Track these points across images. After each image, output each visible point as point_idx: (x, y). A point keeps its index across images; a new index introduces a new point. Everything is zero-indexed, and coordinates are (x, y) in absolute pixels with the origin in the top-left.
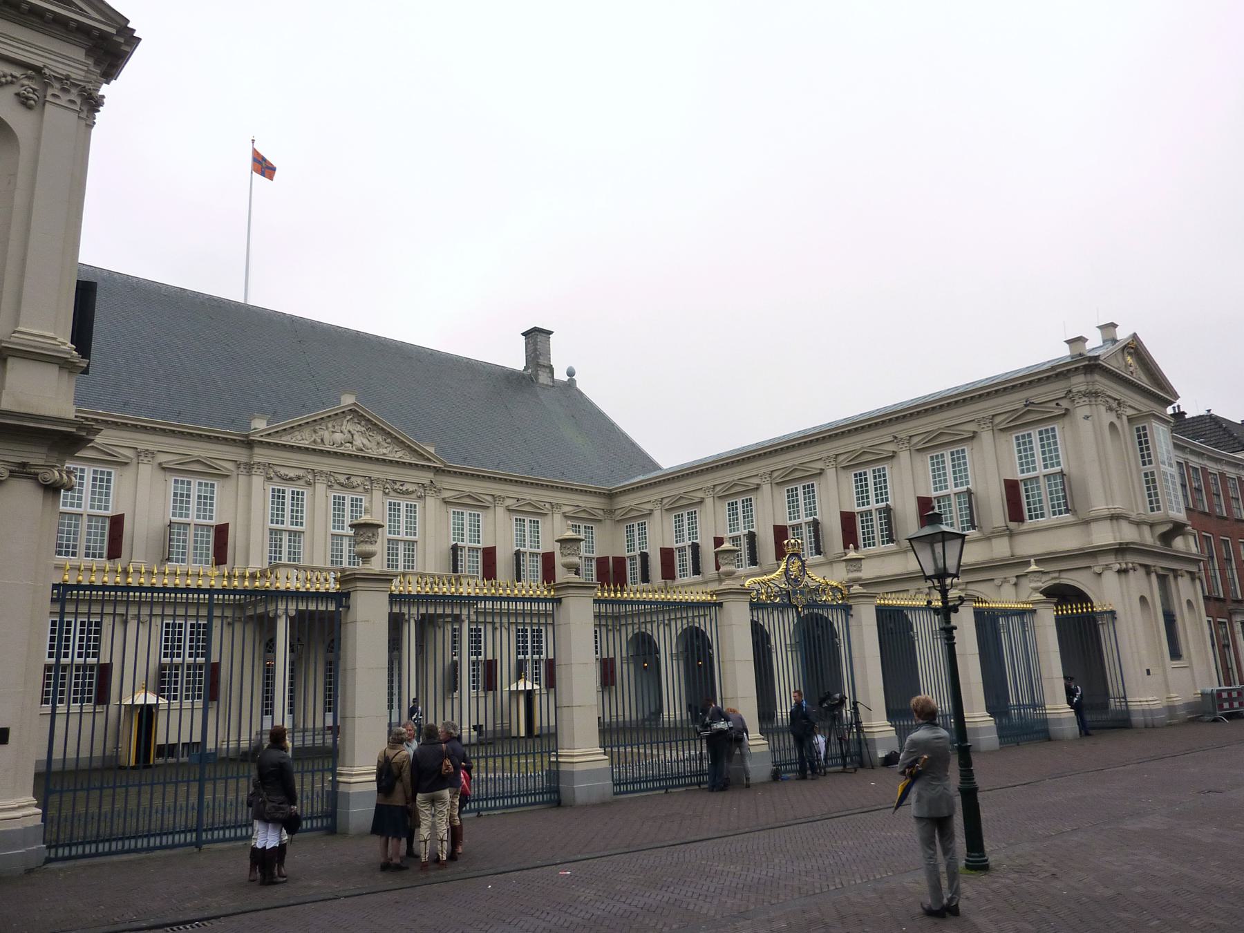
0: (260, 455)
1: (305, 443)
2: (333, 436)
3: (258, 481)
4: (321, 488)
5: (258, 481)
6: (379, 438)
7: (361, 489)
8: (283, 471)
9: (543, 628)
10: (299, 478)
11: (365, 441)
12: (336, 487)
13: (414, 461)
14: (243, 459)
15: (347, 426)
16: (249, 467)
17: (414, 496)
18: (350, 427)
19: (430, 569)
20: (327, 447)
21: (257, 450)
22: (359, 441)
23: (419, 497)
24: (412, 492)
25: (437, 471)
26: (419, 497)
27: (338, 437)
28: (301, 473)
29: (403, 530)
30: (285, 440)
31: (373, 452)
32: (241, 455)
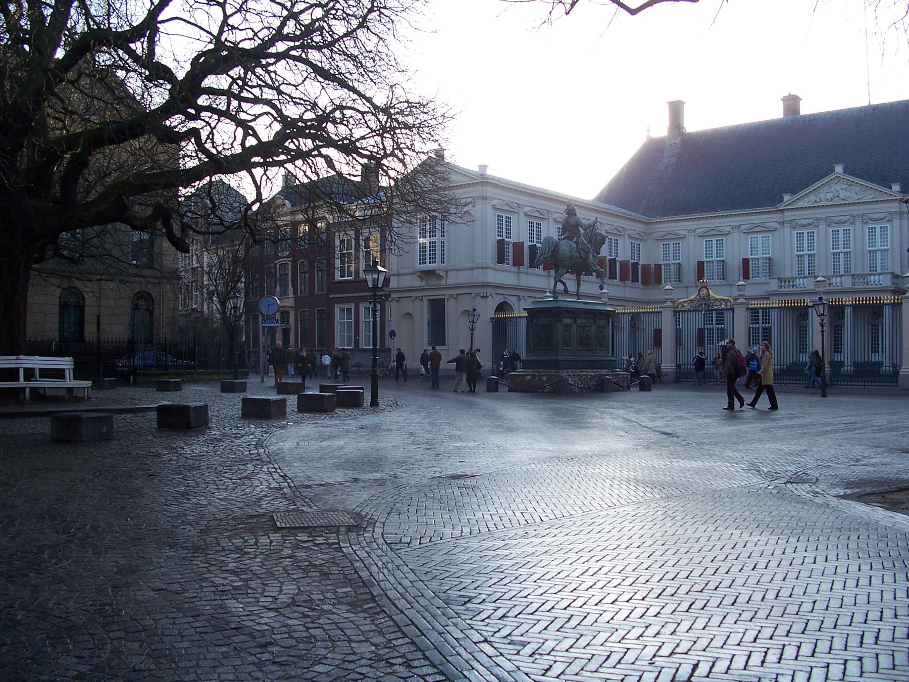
0: (788, 216)
3: (787, 230)
4: (822, 227)
5: (787, 230)
6: (858, 188)
8: (800, 222)
11: (849, 194)
14: (779, 220)
16: (783, 223)
18: (837, 187)
21: (786, 214)
24: (882, 219)
26: (889, 221)
27: (829, 196)
28: (810, 221)
30: (800, 204)
32: (777, 217)
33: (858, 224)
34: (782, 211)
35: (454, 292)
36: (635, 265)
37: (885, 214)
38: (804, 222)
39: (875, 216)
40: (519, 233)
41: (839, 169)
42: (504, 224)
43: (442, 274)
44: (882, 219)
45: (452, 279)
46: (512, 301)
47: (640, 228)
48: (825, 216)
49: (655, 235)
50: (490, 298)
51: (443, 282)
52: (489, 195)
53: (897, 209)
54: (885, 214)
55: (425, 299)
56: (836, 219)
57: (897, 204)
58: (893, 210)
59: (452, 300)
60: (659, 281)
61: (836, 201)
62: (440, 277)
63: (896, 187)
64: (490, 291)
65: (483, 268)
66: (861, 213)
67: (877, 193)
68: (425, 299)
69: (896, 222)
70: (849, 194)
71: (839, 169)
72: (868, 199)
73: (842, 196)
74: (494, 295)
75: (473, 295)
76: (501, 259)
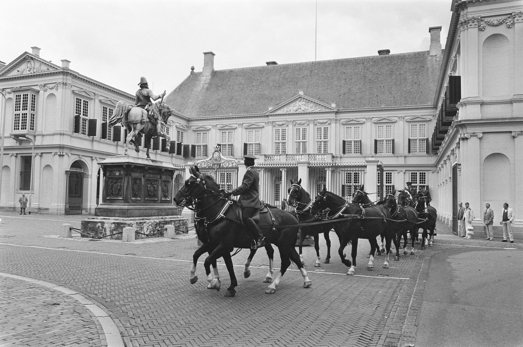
0: (271, 119)
1: (284, 113)
2: (292, 108)
5: (270, 127)
7: (306, 125)
8: (278, 123)
9: (360, 172)
10: (283, 124)
11: (306, 108)
12: (297, 125)
13: (324, 110)
14: (267, 121)
15: (298, 103)
17: (327, 124)
18: (300, 103)
19: (311, 152)
20: (292, 112)
21: (270, 118)
22: (303, 108)
23: (329, 124)
24: (325, 123)
25: (337, 113)
26: (329, 124)
27: (295, 108)
28: (283, 123)
30: (279, 112)
31: (310, 110)
32: (265, 120)
33: (311, 125)
34: (267, 116)
35: (39, 151)
36: (179, 145)
37: (327, 120)
38: (280, 123)
39: (321, 121)
42: (81, 105)
43: (31, 138)
44: (325, 123)
45: (39, 141)
46: (87, 161)
47: (184, 123)
48: (292, 120)
49: (192, 128)
50: (66, 156)
51: (31, 144)
52: (68, 82)
53: (334, 118)
54: (327, 120)
55: (19, 156)
56: (298, 122)
57: (334, 115)
58: (332, 118)
59: (38, 158)
60: (194, 155)
61: (299, 111)
62: (29, 141)
63: (334, 105)
64: (65, 151)
65: (61, 134)
66: (313, 119)
67: (323, 108)
68: (19, 156)
69: (333, 125)
70: (306, 108)
72: (318, 110)
73: (303, 108)
74: (70, 155)
75: (53, 154)
76: (77, 130)
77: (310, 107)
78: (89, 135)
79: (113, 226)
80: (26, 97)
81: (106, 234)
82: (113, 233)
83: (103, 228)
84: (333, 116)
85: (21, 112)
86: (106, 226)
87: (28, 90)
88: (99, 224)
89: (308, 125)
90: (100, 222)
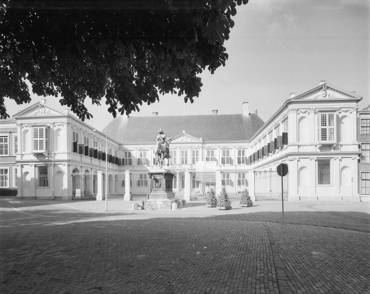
15: (182, 138)
20: (179, 142)
27: (181, 140)
29: (195, 155)
38: (173, 148)
40: (81, 142)
41: (184, 132)
44: (197, 148)
51: (47, 158)
61: (183, 142)
62: (44, 156)
63: (201, 139)
71: (184, 132)
77: (189, 140)
78: (80, 153)
79: (162, 203)
80: (41, 131)
81: (158, 207)
82: (162, 206)
83: (155, 204)
84: (201, 145)
85: (39, 139)
86: (157, 203)
87: (44, 126)
88: (153, 203)
89: (188, 149)
90: (153, 201)
